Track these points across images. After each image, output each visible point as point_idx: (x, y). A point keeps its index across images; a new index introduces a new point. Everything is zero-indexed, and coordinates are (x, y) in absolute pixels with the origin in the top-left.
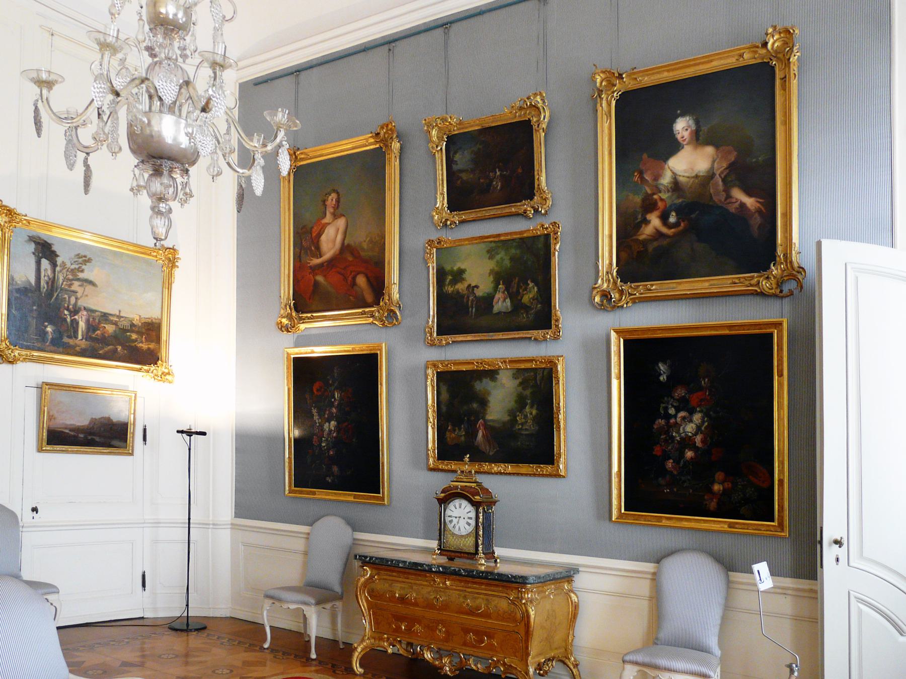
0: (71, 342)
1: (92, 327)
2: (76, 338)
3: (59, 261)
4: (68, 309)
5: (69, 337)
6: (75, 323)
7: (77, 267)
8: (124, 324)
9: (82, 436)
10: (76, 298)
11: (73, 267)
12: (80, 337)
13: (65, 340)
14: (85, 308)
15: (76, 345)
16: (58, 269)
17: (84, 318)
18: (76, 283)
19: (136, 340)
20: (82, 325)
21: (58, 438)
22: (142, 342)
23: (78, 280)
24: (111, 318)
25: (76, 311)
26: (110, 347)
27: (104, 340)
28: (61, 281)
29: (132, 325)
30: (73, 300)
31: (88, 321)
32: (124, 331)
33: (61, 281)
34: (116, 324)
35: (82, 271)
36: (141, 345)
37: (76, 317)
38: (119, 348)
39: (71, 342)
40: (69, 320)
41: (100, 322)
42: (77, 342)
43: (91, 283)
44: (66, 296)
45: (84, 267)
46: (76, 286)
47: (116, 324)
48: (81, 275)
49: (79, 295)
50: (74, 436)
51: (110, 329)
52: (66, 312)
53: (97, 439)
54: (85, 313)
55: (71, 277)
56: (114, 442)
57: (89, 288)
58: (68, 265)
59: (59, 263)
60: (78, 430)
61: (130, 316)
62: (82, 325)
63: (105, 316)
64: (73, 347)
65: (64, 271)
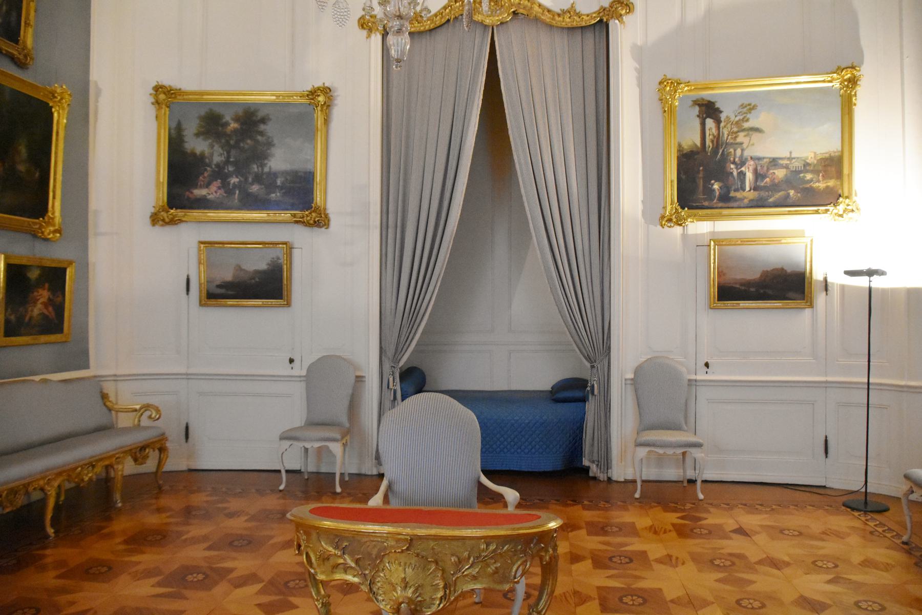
0: (738, 195)
1: (758, 175)
2: (744, 190)
3: (723, 117)
4: (734, 162)
5: (736, 190)
6: (742, 175)
7: (741, 117)
8: (797, 165)
9: (752, 290)
10: (743, 150)
11: (737, 119)
12: (748, 188)
13: (732, 194)
14: (751, 158)
15: (745, 198)
16: (722, 125)
17: (751, 168)
18: (741, 134)
19: (811, 180)
20: (749, 176)
21: (730, 292)
22: (819, 181)
23: (743, 130)
24: (781, 162)
25: (743, 163)
26: (782, 193)
27: (775, 187)
28: (726, 136)
29: (806, 164)
30: (739, 152)
31: (755, 172)
32: (797, 172)
33: (726, 136)
34: (787, 167)
35: (747, 120)
36: (817, 184)
37: (743, 169)
38: (792, 192)
39: (738, 195)
40: (735, 173)
41: (768, 169)
42: (745, 194)
43: (757, 130)
44: (732, 150)
45: (748, 116)
46: (741, 138)
47: (787, 167)
48: (746, 125)
49: (745, 146)
50: (745, 290)
51: (780, 174)
52: (732, 166)
53: (770, 292)
54: (752, 163)
55: (735, 129)
56: (790, 294)
57: (755, 136)
58: (733, 118)
59: (722, 119)
60: (749, 284)
61: (803, 155)
62: (749, 176)
63: (774, 162)
64: (742, 200)
65: (729, 125)
